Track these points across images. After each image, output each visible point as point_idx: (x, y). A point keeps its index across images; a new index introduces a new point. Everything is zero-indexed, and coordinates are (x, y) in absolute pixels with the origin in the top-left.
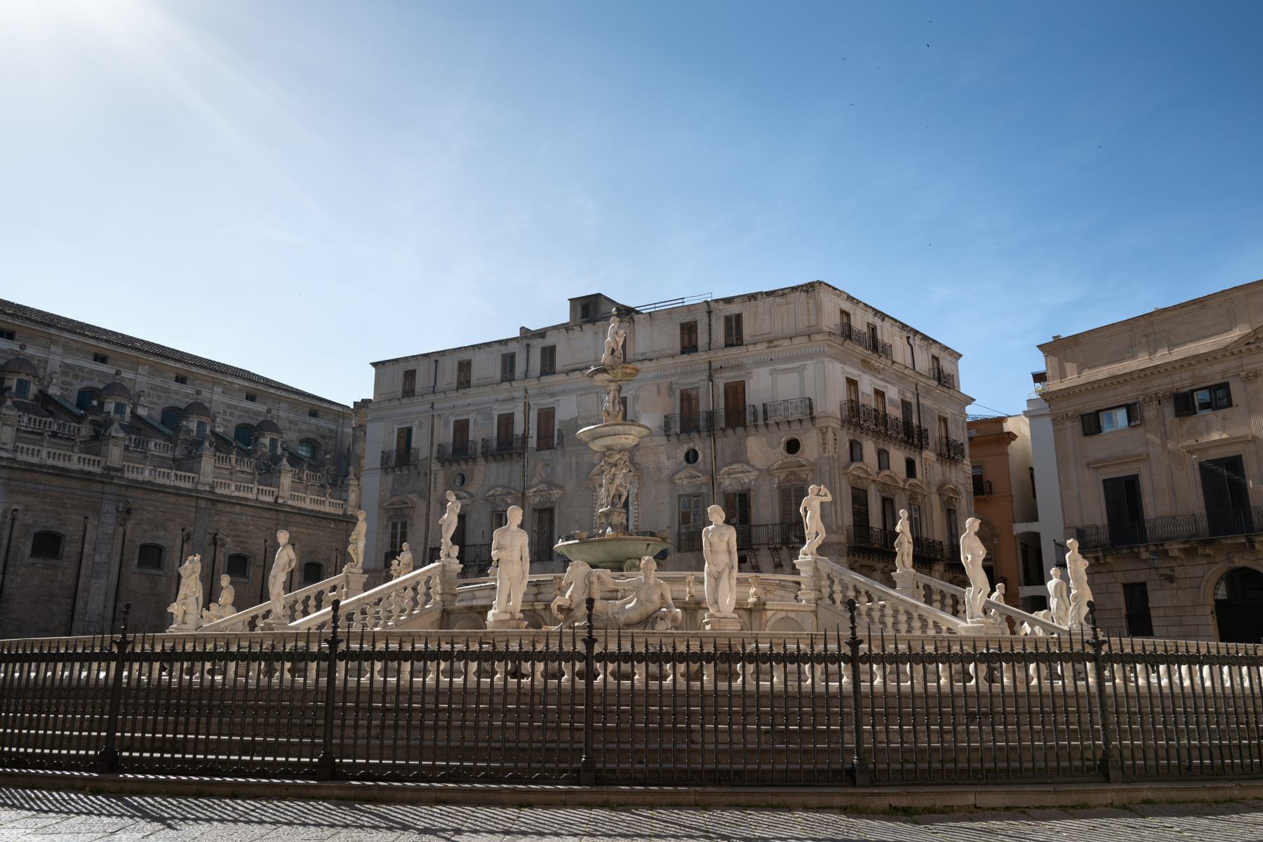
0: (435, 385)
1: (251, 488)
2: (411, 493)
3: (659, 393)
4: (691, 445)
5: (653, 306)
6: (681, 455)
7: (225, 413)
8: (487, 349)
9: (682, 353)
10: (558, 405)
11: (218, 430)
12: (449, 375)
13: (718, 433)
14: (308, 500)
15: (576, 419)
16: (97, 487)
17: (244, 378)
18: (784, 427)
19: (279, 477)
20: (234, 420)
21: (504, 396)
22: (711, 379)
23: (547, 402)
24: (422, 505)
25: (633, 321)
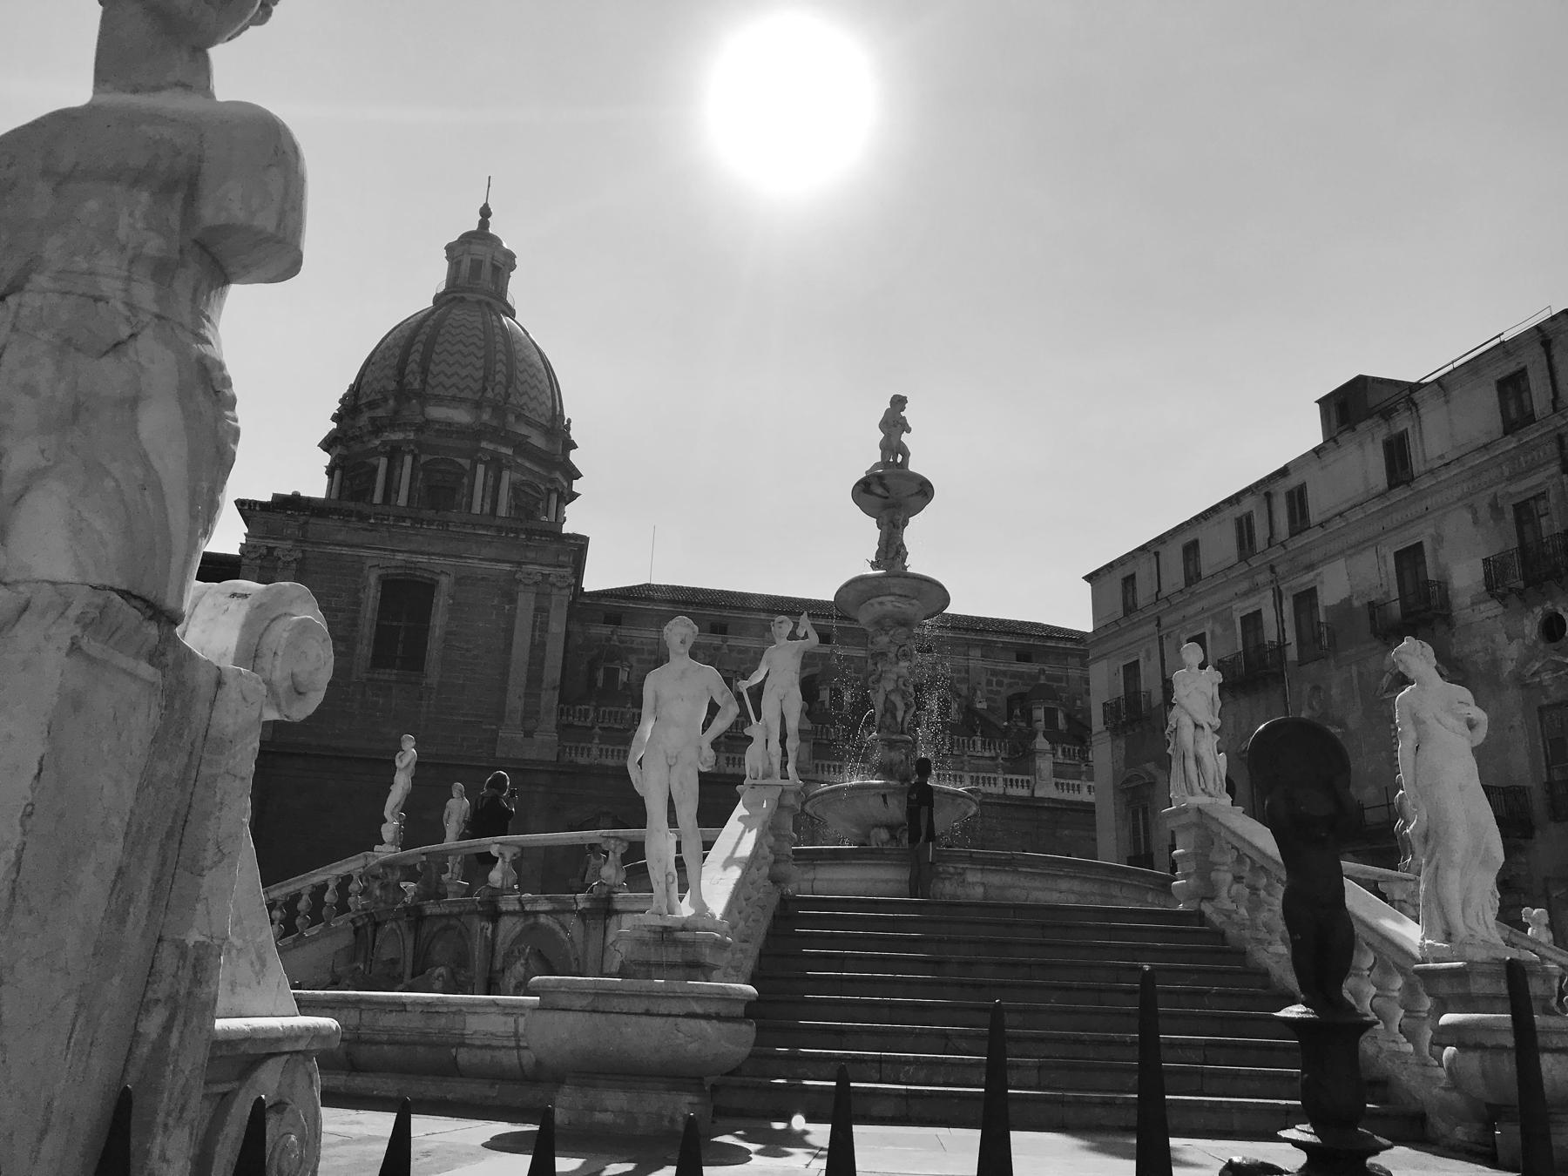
0: (1159, 590)
1: (995, 779)
2: (1148, 762)
3: (1475, 522)
4: (1549, 605)
5: (1450, 368)
6: (1531, 626)
7: (989, 683)
8: (1215, 518)
9: (1506, 433)
10: (1322, 582)
11: (979, 706)
12: (1174, 575)
14: (1085, 790)
15: (1348, 601)
17: (1007, 633)
19: (1033, 760)
20: (1002, 690)
21: (1244, 586)
23: (1306, 579)
25: (1415, 405)
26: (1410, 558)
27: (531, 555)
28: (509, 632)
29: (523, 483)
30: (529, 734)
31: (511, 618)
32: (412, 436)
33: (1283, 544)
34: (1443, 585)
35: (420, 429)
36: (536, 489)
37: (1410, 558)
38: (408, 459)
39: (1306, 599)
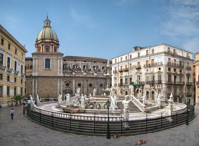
6: (146, 70)
13: (151, 67)
16: (84, 78)
18: (159, 66)
22: (150, 59)
23: (131, 63)
24: (118, 78)
26: (139, 63)
27: (59, 56)
28: (57, 64)
29: (55, 47)
30: (60, 73)
31: (57, 62)
32: (44, 43)
33: (129, 60)
34: (141, 66)
35: (45, 42)
36: (56, 47)
37: (139, 63)
38: (44, 46)
39: (131, 64)
